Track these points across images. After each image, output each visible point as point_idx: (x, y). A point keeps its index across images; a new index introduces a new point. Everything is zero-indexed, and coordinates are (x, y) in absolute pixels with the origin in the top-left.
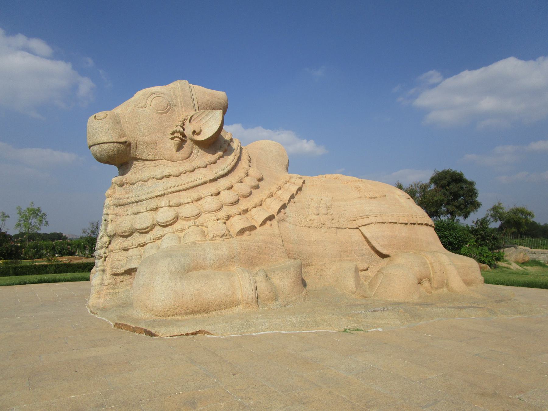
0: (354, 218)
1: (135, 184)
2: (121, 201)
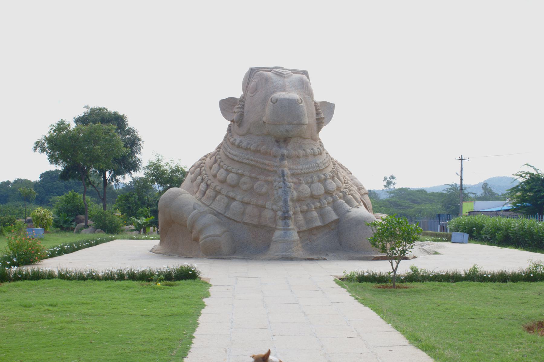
2: (297, 171)
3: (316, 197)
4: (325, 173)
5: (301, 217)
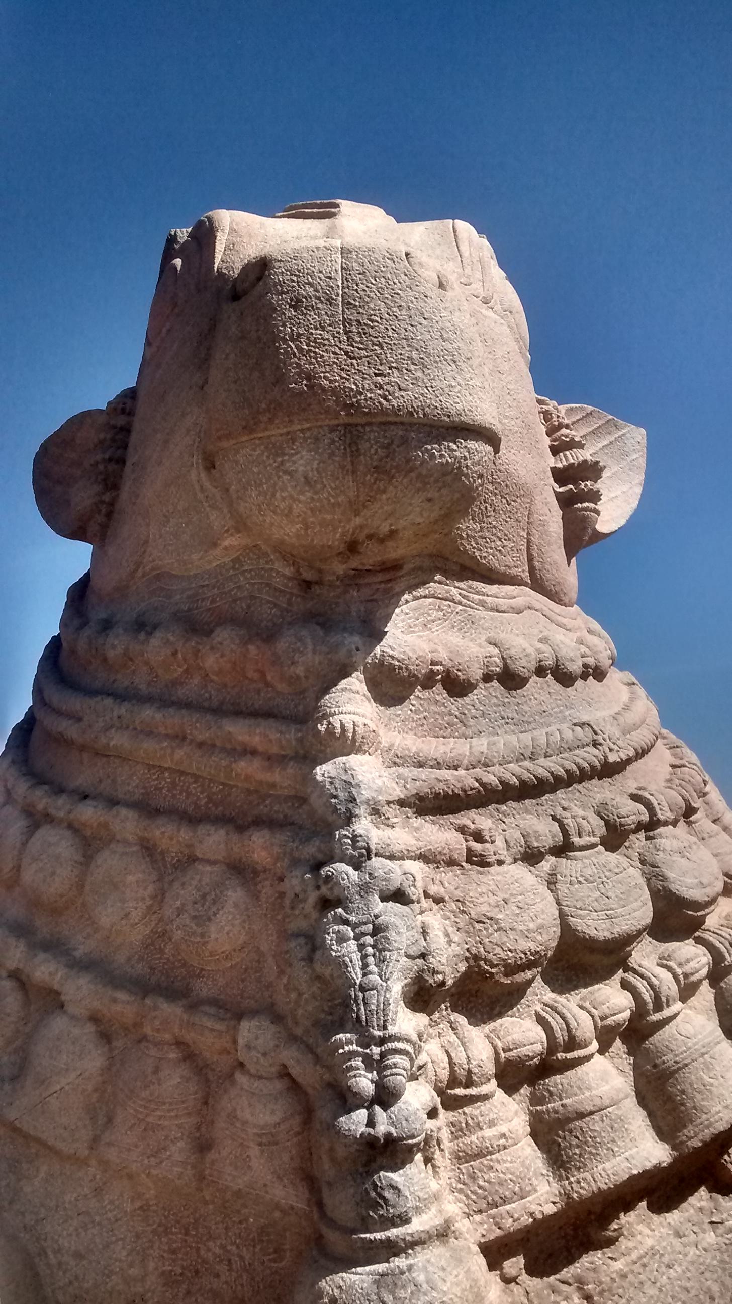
4: (640, 789)
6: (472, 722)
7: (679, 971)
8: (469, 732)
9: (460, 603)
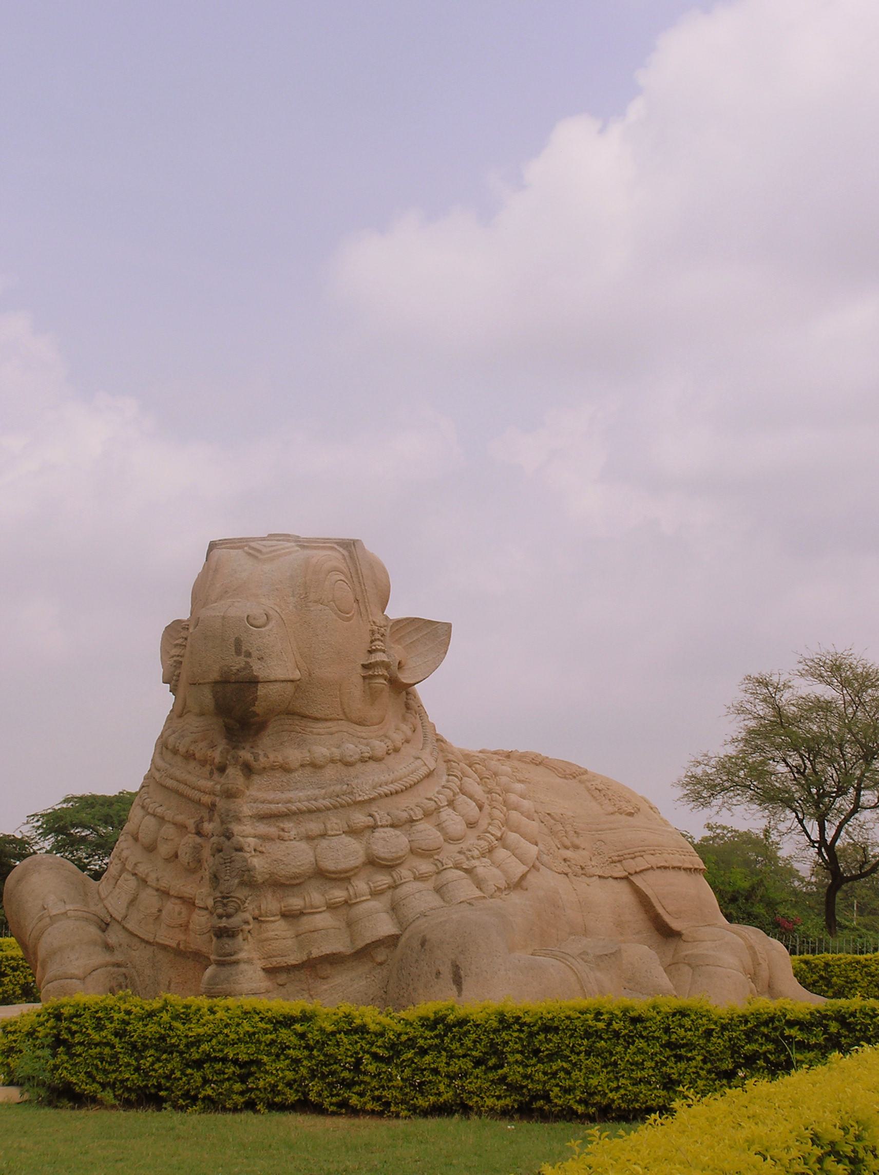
0: (619, 856)
1: (296, 770)
2: (273, 806)
3: (334, 876)
5: (278, 928)
6: (293, 784)
7: (372, 885)
8: (292, 789)
9: (300, 733)
